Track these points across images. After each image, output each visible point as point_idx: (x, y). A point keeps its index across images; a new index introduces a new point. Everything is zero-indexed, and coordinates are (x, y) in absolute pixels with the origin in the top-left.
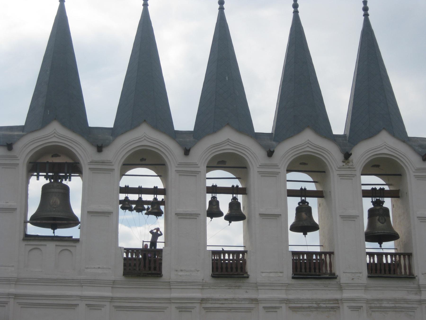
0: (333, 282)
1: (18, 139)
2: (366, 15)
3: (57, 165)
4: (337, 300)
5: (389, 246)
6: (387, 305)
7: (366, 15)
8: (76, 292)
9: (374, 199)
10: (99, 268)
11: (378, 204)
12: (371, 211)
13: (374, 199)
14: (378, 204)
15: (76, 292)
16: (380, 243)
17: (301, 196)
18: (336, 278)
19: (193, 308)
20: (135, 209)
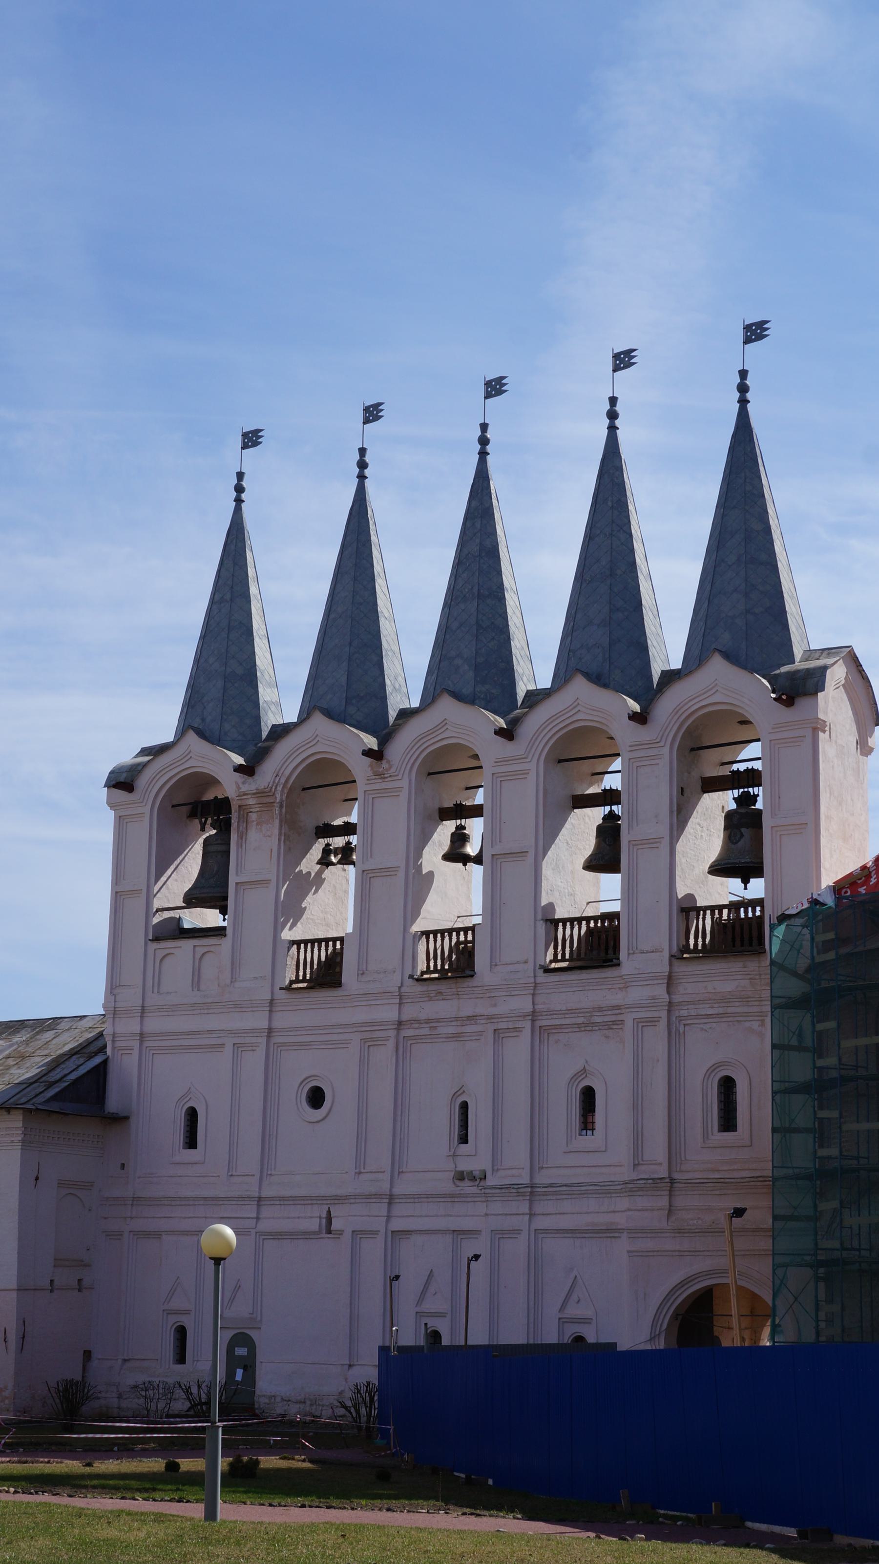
0: (609, 973)
1: (140, 772)
2: (743, 402)
3: (200, 808)
4: (618, 1007)
5: (757, 888)
6: (711, 1011)
7: (743, 402)
8: (215, 1022)
9: (736, 793)
10: (256, 978)
11: (746, 800)
12: (729, 816)
13: (736, 793)
14: (746, 800)
15: (215, 1022)
16: (746, 882)
17: (604, 805)
18: (619, 965)
19: (387, 1039)
20: (339, 862)
